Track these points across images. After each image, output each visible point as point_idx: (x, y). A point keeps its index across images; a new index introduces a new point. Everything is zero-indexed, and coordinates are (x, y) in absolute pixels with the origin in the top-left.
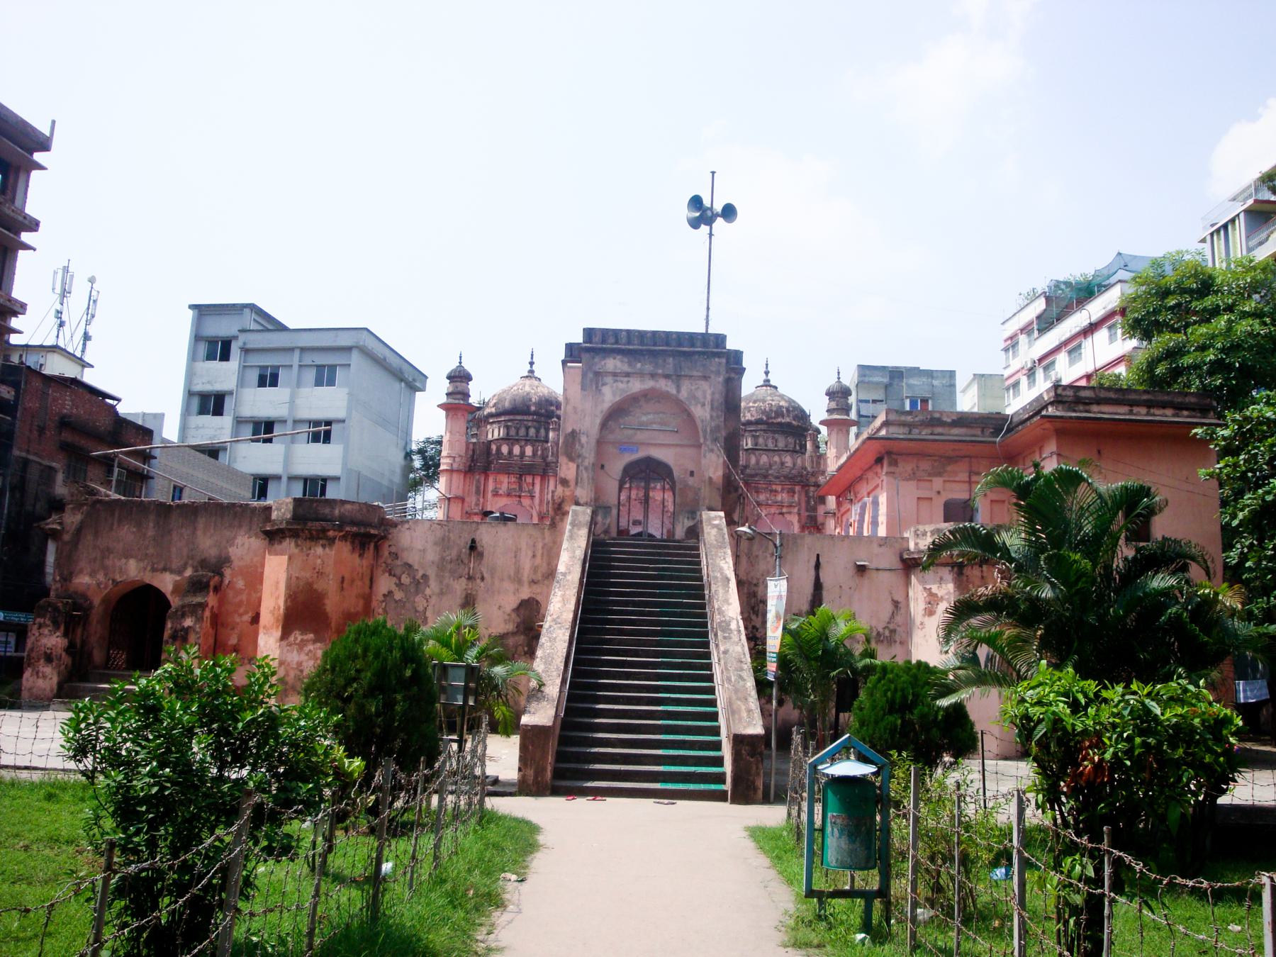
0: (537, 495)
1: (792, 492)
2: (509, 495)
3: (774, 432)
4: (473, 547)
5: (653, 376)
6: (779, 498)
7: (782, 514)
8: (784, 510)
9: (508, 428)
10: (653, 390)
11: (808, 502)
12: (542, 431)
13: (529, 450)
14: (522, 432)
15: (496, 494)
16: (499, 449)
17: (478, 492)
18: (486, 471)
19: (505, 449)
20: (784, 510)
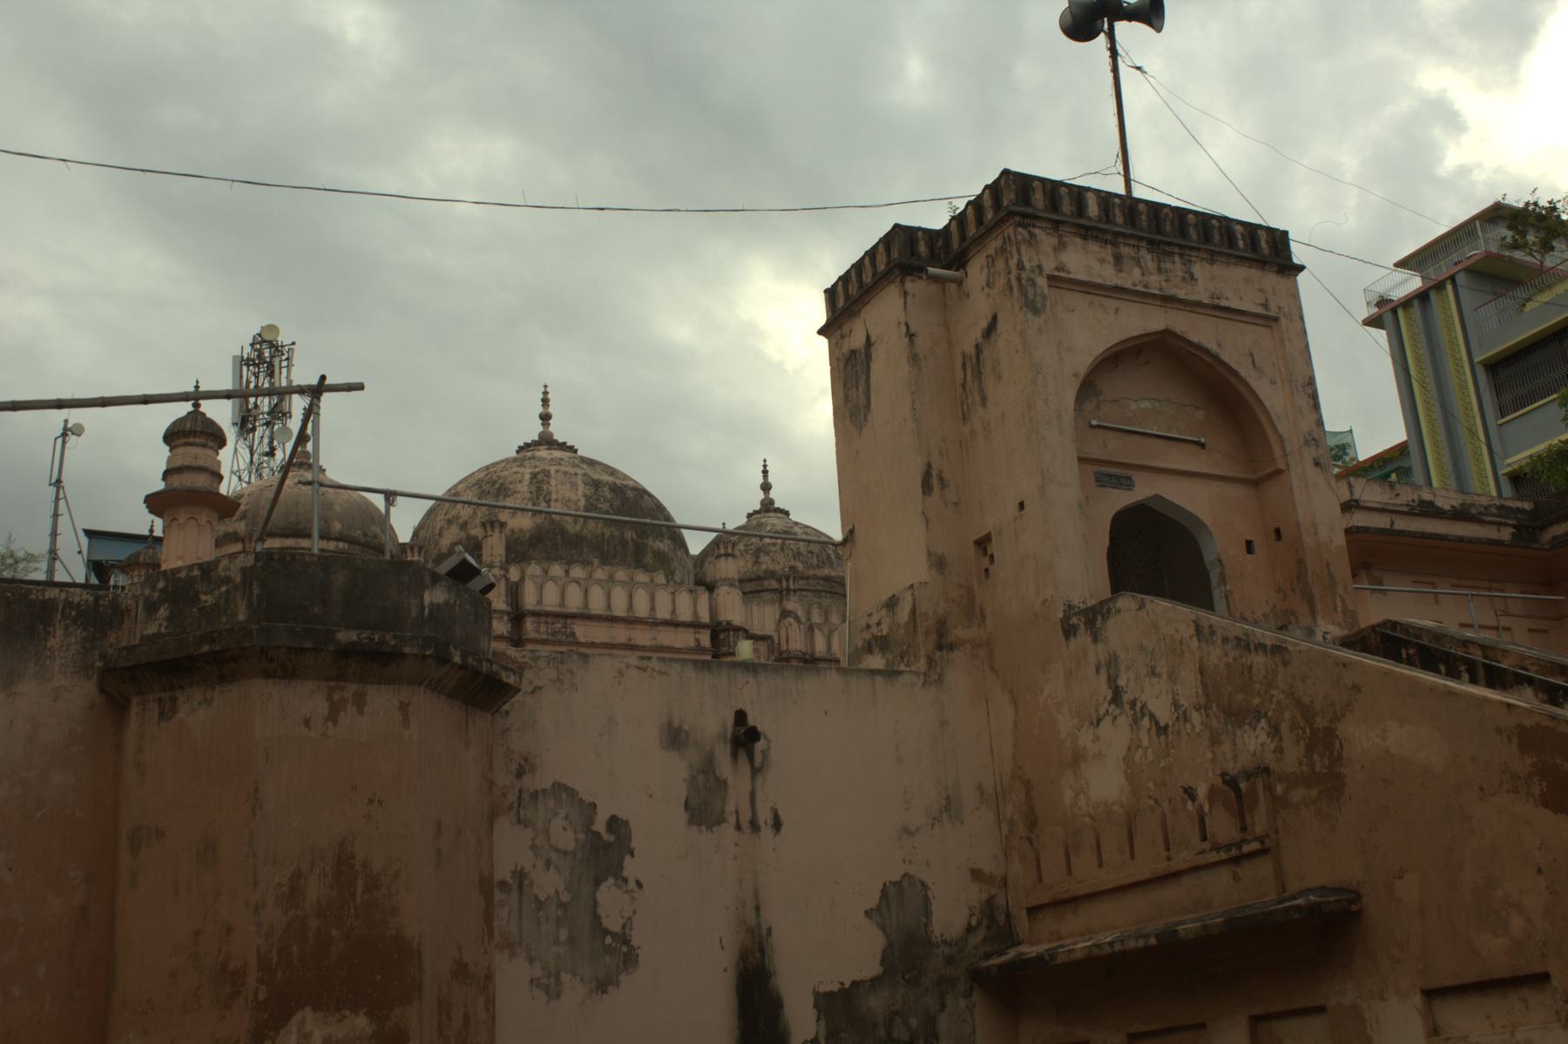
4: (745, 737)
5: (1167, 300)
10: (1167, 332)
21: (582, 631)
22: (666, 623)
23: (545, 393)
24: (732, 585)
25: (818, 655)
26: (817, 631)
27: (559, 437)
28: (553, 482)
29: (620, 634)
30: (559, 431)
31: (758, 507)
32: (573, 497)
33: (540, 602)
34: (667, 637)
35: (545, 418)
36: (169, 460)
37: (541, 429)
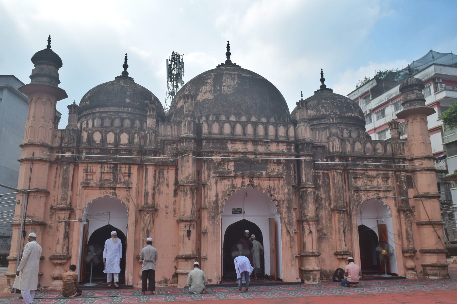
0: (134, 186)
1: (386, 178)
2: (101, 187)
3: (346, 124)
6: (375, 183)
7: (379, 198)
8: (381, 195)
9: (102, 119)
11: (400, 187)
12: (137, 122)
13: (124, 138)
14: (117, 123)
15: (86, 185)
16: (90, 137)
17: (65, 184)
18: (75, 162)
19: (97, 137)
20: (381, 195)
21: (230, 146)
22: (272, 141)
23: (228, 44)
24: (305, 122)
25: (348, 154)
26: (347, 143)
27: (233, 62)
28: (224, 78)
29: (250, 147)
30: (234, 59)
31: (319, 88)
32: (232, 84)
33: (210, 133)
34: (273, 148)
35: (228, 54)
36: (33, 70)
37: (227, 59)
